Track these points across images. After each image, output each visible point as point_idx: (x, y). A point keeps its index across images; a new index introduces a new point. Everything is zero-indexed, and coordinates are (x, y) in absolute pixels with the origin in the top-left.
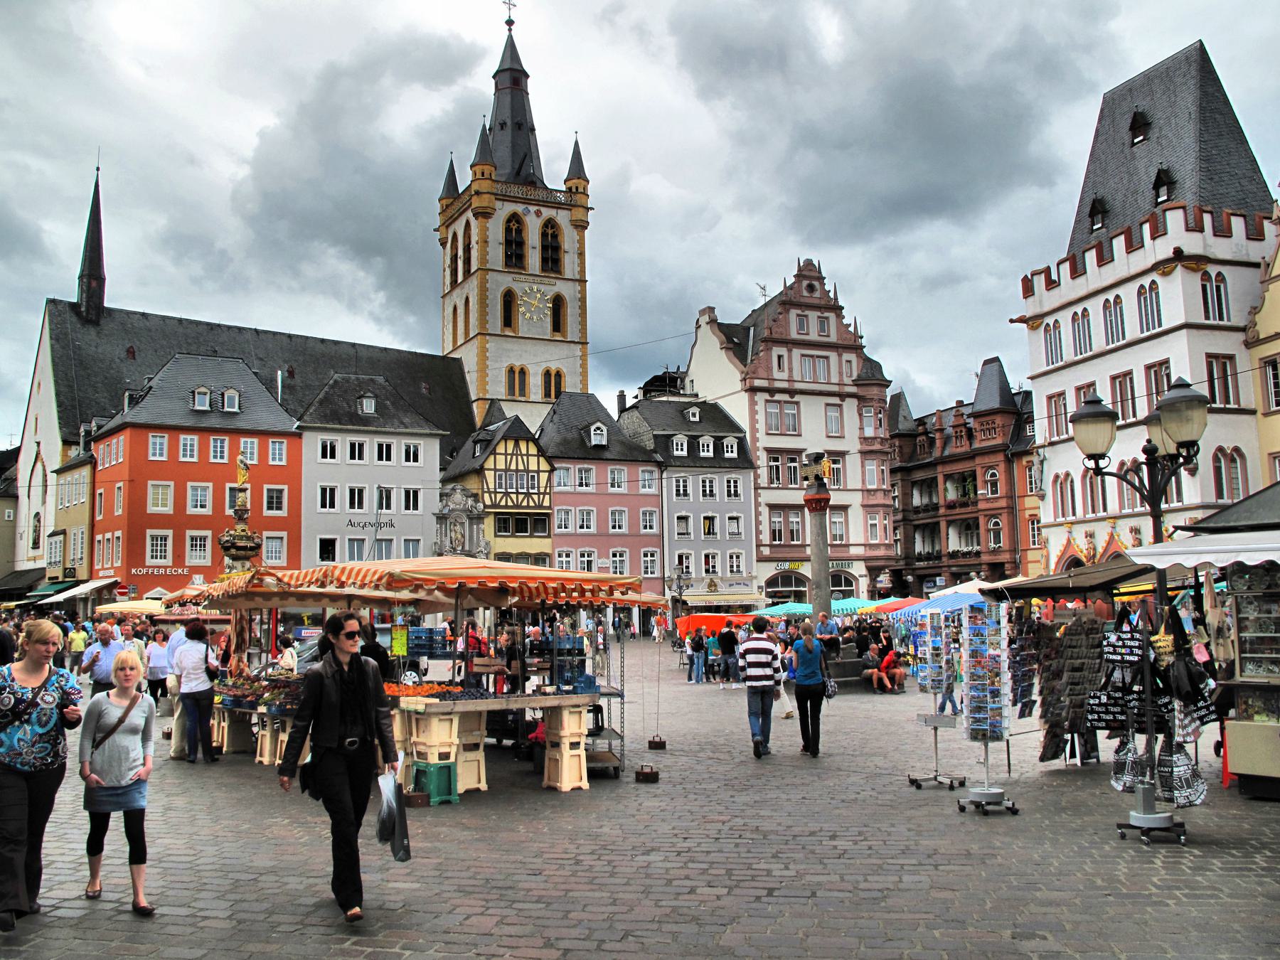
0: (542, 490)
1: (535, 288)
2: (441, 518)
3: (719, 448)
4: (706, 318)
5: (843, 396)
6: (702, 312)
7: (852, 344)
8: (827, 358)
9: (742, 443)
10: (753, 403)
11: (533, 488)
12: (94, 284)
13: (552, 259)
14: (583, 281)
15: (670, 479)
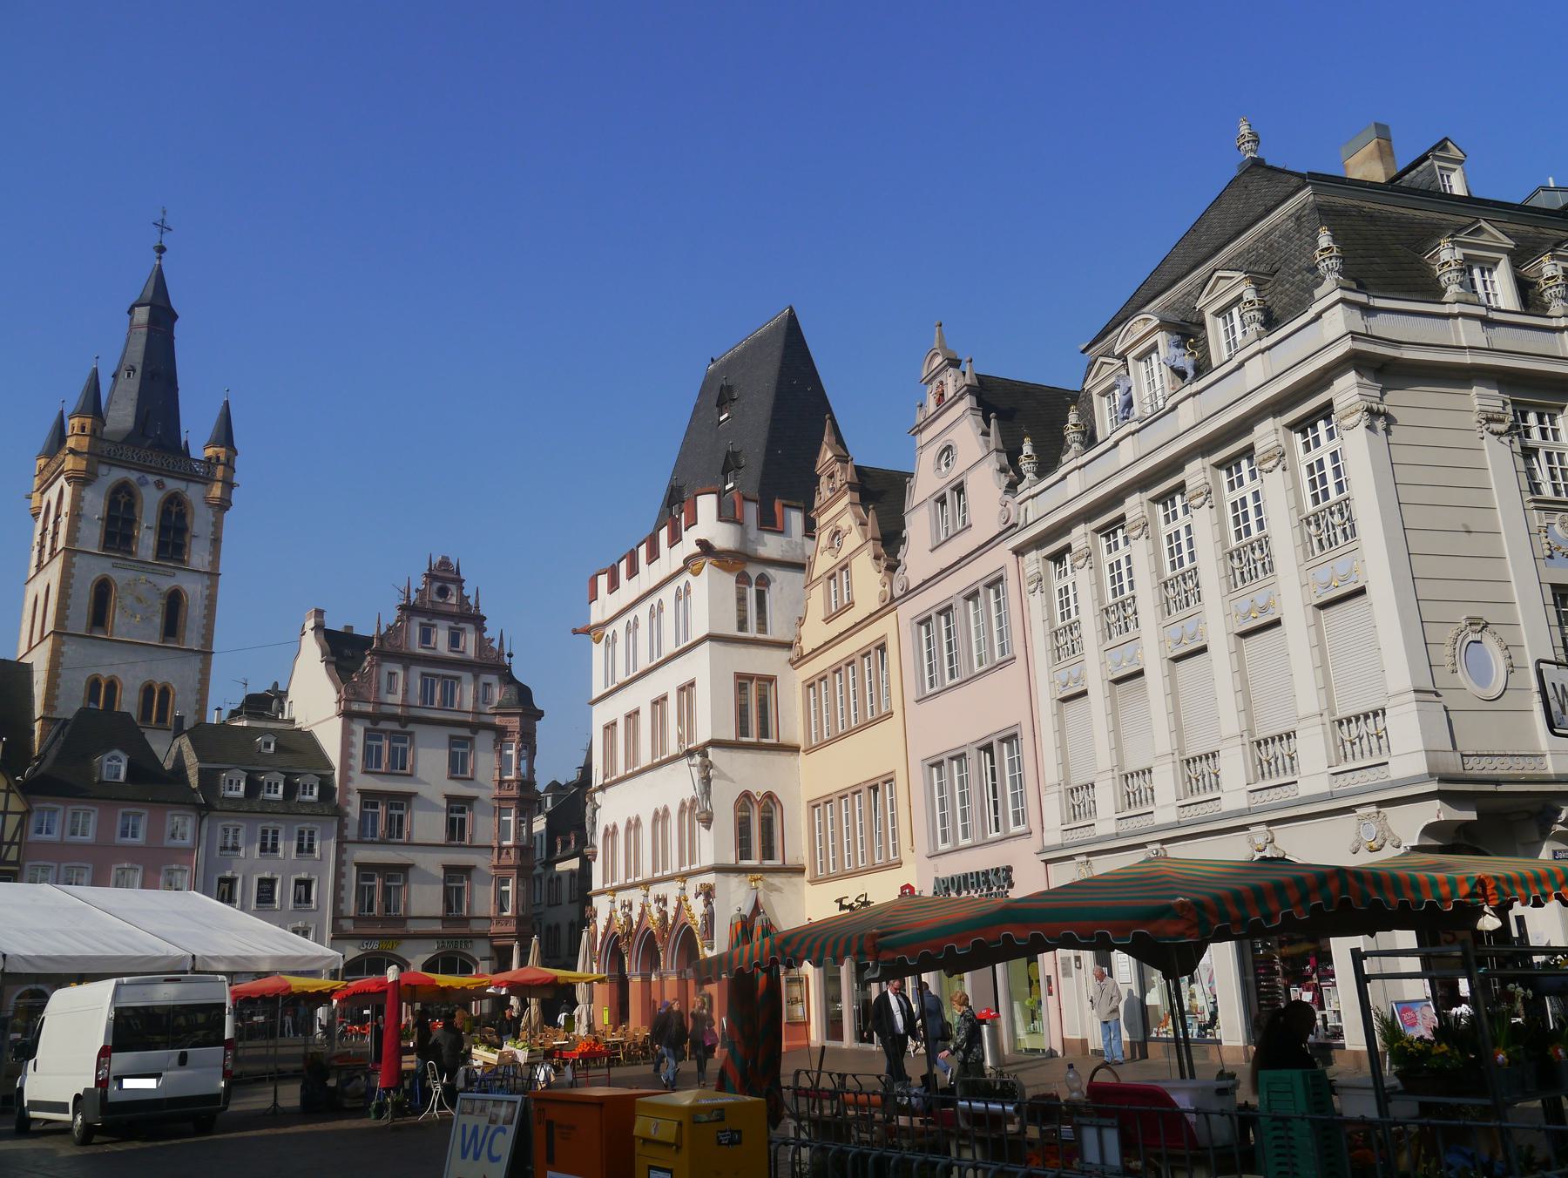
5: (476, 727)
7: (493, 665)
8: (458, 678)
10: (347, 734)
14: (213, 575)
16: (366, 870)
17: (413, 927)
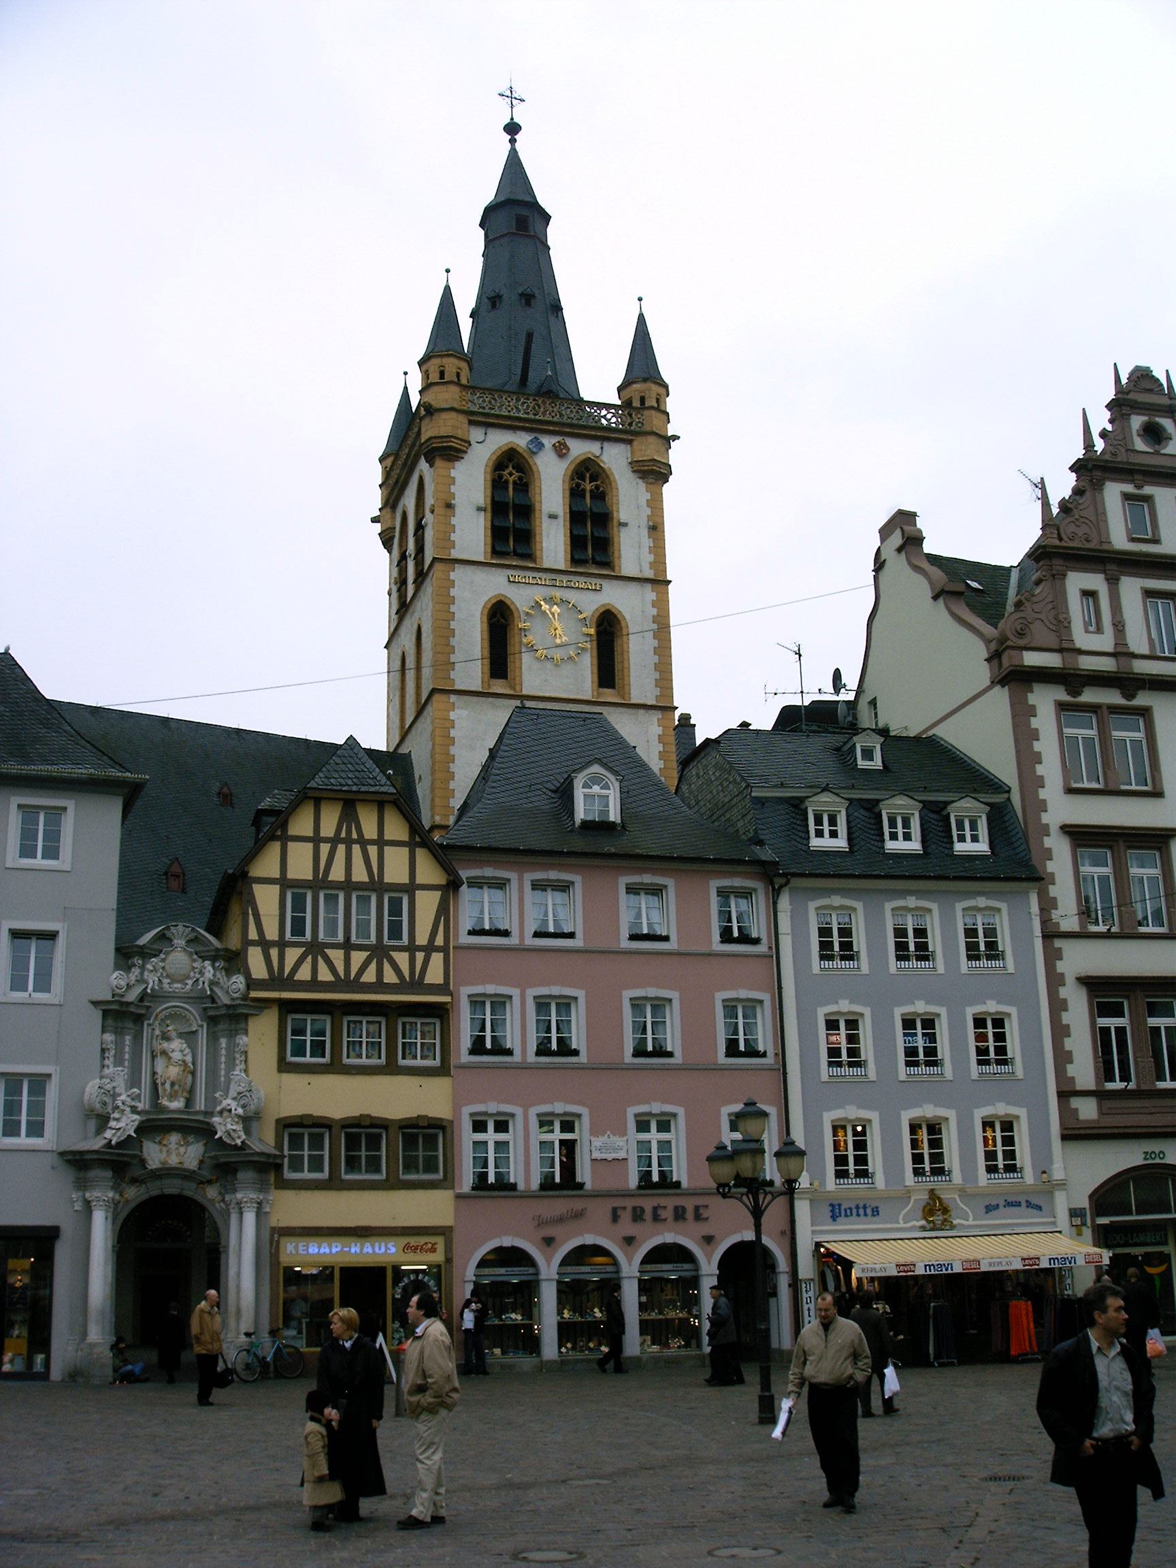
0: (422, 939)
2: (122, 1015)
3: (937, 826)
4: (896, 539)
6: (885, 532)
9: (1001, 821)
10: (1022, 714)
13: (593, 541)
16: (1106, 992)
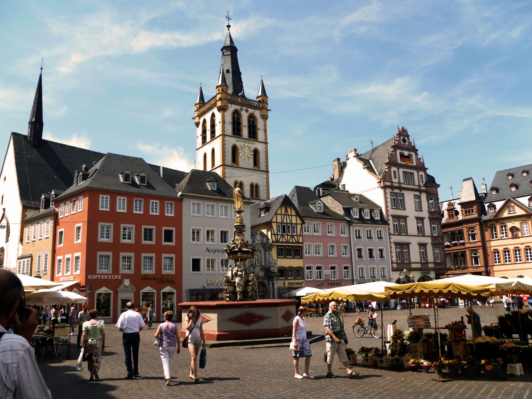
0: (298, 234)
1: (246, 145)
7: (421, 167)
8: (413, 173)
10: (385, 193)
11: (294, 233)
12: (38, 126)
14: (266, 143)
15: (354, 228)
17: (413, 266)
